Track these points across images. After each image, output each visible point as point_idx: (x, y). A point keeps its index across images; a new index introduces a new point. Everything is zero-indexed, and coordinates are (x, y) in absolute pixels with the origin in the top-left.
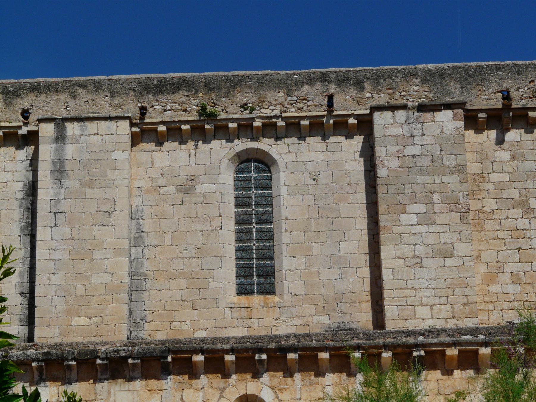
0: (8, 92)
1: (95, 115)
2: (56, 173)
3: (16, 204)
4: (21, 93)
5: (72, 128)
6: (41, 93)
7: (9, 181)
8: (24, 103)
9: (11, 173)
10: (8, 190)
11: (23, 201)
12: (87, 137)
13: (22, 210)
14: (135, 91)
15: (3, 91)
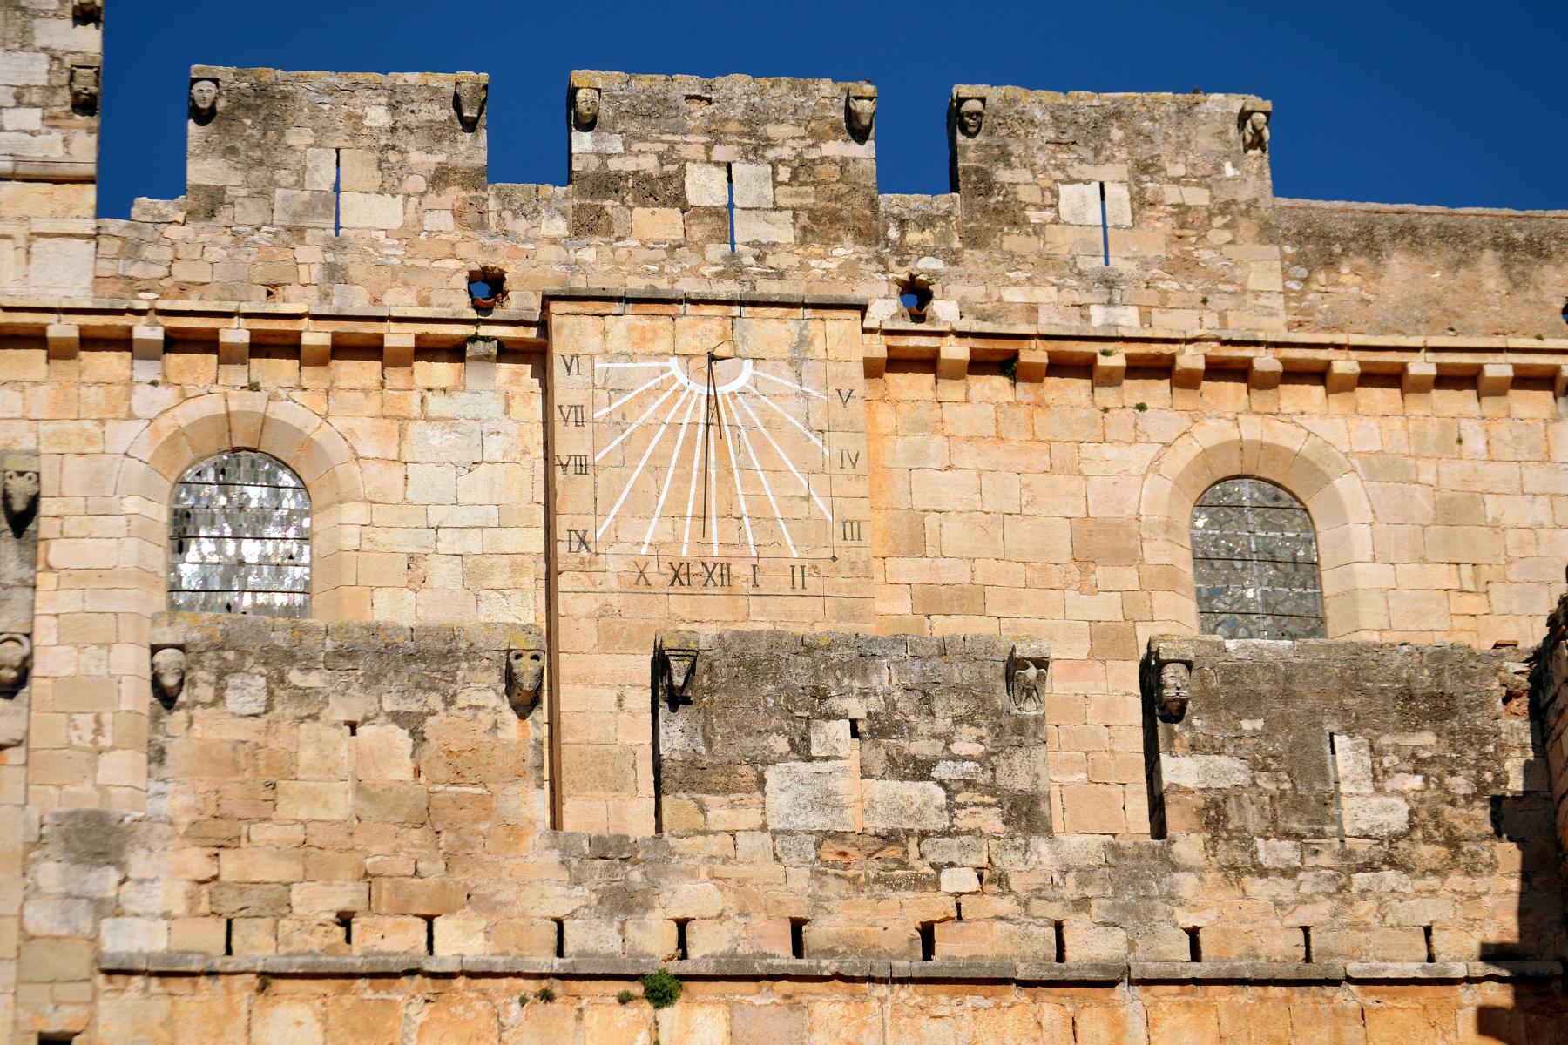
0: (1511, 245)
4: (1553, 248)
7: (1542, 526)
9: (1546, 499)
10: (1543, 554)
15: (1493, 239)
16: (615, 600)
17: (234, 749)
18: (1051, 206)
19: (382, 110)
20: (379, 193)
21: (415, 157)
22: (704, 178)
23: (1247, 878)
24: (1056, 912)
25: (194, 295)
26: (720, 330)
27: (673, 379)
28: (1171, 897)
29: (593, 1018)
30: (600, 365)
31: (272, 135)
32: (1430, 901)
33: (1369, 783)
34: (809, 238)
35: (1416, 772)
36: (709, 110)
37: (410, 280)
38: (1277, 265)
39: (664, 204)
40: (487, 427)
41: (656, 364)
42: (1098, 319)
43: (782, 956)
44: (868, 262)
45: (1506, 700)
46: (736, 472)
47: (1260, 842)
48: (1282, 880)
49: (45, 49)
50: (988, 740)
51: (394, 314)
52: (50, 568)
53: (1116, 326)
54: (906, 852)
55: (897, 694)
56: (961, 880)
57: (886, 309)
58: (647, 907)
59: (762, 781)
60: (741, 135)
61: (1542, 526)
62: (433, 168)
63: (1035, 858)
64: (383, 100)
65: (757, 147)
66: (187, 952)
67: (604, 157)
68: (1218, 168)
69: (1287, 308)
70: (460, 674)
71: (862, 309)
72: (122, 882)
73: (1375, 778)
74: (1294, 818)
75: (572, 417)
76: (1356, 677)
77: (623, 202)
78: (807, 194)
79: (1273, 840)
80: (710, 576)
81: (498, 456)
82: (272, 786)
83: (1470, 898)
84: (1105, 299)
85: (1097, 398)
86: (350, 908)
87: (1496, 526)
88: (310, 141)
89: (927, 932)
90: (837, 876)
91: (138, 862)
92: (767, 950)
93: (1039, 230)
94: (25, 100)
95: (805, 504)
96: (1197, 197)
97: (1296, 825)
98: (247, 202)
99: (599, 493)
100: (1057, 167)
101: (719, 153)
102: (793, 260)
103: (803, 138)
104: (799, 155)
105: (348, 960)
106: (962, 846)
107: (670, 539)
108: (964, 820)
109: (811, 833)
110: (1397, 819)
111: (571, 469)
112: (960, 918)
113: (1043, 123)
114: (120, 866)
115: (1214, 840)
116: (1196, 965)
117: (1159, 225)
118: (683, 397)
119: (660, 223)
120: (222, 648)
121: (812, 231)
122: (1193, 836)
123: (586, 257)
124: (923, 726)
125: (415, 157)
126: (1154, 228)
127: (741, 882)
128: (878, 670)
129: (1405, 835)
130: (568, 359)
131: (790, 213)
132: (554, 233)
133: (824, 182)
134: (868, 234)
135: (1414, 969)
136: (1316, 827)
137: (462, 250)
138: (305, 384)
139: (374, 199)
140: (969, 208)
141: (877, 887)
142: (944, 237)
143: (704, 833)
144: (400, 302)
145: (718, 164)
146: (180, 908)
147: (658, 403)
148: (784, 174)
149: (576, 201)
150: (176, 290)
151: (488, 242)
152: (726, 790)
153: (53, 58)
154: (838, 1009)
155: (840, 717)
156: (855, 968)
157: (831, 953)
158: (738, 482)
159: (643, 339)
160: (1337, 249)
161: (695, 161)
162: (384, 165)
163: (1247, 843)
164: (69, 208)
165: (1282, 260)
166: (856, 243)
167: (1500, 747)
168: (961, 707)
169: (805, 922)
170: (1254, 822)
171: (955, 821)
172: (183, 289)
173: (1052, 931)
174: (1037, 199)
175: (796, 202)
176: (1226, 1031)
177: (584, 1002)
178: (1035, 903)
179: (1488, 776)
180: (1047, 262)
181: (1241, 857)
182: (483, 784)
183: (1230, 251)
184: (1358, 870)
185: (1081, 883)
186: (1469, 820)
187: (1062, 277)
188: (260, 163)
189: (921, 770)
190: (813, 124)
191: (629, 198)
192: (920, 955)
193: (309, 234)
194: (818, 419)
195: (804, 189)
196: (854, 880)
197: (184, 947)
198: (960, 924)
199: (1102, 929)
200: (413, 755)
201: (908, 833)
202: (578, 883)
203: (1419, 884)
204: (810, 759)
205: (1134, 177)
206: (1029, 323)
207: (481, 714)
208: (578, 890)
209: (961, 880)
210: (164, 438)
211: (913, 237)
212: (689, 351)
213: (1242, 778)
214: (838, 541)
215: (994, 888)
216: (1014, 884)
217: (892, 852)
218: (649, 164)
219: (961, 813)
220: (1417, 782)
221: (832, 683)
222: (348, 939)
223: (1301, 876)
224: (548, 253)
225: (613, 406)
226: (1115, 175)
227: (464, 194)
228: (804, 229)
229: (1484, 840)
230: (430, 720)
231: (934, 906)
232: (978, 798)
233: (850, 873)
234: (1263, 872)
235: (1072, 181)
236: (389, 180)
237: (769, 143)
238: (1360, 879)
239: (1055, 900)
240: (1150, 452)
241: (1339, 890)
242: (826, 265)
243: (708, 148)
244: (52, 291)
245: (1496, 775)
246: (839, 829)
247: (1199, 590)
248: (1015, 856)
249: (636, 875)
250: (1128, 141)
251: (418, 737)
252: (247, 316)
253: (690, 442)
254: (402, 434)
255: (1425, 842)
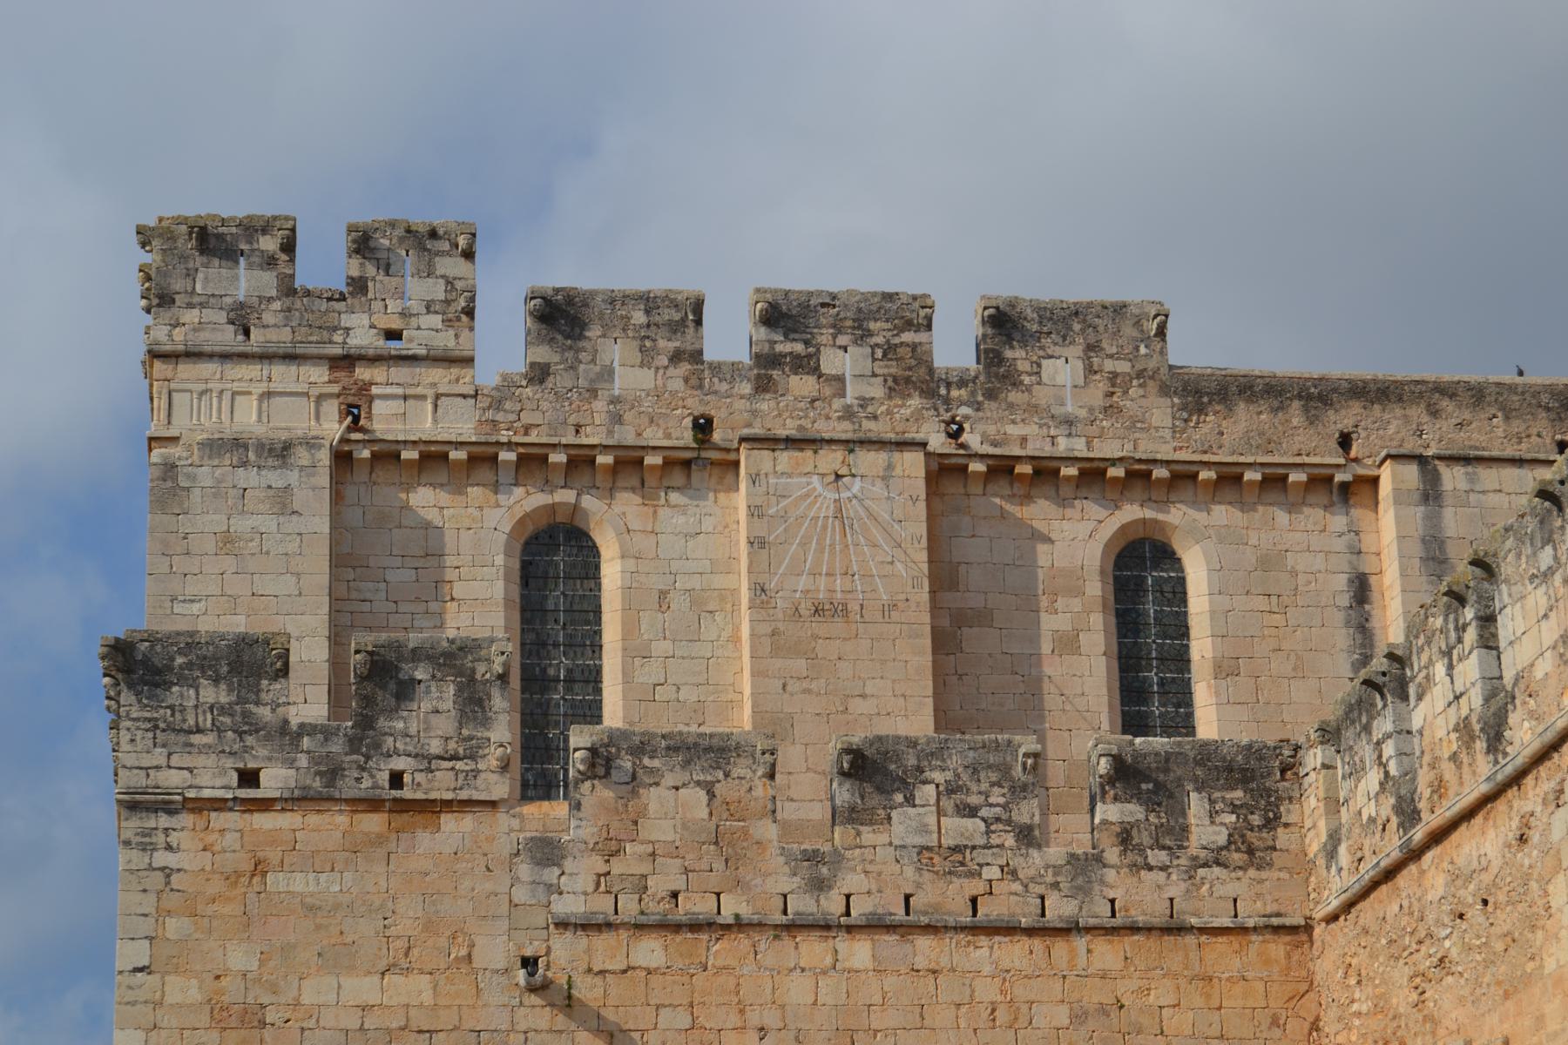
0: (1310, 397)
1: (1486, 454)
2: (1431, 563)
3: (1340, 617)
5: (1453, 478)
6: (1373, 403)
7: (1320, 572)
8: (1343, 417)
11: (1350, 612)
12: (1481, 495)
13: (1351, 631)
14: (1548, 409)
16: (782, 627)
17: (616, 802)
18: (1037, 373)
19: (641, 313)
20: (640, 366)
21: (662, 343)
22: (832, 356)
23: (1143, 873)
24: (1040, 889)
25: (534, 432)
26: (841, 458)
27: (815, 489)
28: (1102, 882)
29: (804, 947)
30: (772, 481)
31: (577, 330)
32: (1237, 884)
33: (1207, 818)
34: (893, 394)
35: (1233, 813)
36: (834, 311)
37: (661, 422)
38: (1169, 410)
39: (808, 373)
40: (704, 511)
41: (804, 480)
42: (1063, 446)
43: (899, 914)
44: (927, 409)
45: (1283, 772)
46: (851, 547)
47: (1149, 851)
48: (1161, 873)
49: (442, 277)
50: (1008, 796)
51: (651, 444)
52: (453, 599)
53: (1073, 450)
54: (964, 858)
55: (960, 770)
56: (992, 873)
57: (938, 441)
58: (830, 888)
59: (889, 818)
60: (854, 328)
61: (1320, 572)
62: (672, 350)
63: (1031, 861)
64: (642, 307)
65: (862, 335)
66: (596, 913)
67: (773, 343)
68: (1137, 349)
69: (1173, 438)
70: (732, 759)
71: (924, 445)
72: (563, 873)
73: (1211, 816)
74: (1168, 838)
75: (756, 513)
76: (1202, 759)
77: (784, 373)
78: (891, 366)
79: (1156, 851)
80: (836, 611)
81: (710, 529)
82: (636, 823)
83: (1258, 882)
84: (1067, 432)
85: (1061, 492)
86: (678, 888)
87: (1294, 573)
88: (599, 333)
89: (974, 901)
90: (928, 870)
91: (569, 865)
92: (892, 911)
93: (1029, 389)
94: (432, 309)
95: (890, 566)
96: (1123, 367)
97: (1168, 842)
98: (563, 373)
99: (772, 561)
100: (1042, 348)
101: (843, 340)
102: (883, 408)
103: (889, 330)
104: (888, 341)
105: (678, 918)
106: (993, 854)
107: (813, 588)
108: (995, 840)
109: (914, 847)
110: (1222, 839)
111: (756, 545)
112: (991, 893)
113: (1033, 319)
114: (559, 865)
115: (1125, 850)
116: (1113, 920)
117: (1101, 384)
118: (820, 499)
119: (802, 385)
120: (608, 746)
121: (895, 390)
122: (1114, 848)
123: (762, 407)
124: (974, 788)
125: (662, 343)
126: (1098, 388)
127: (879, 874)
128: (950, 756)
129: (1226, 848)
130: (754, 476)
131: (882, 378)
132: (742, 392)
133: (902, 359)
134: (929, 392)
135: (1226, 922)
136: (1179, 843)
137: (689, 402)
138: (598, 485)
139: (638, 371)
140: (988, 374)
141: (948, 877)
142: (973, 393)
143: (861, 847)
144: (653, 437)
145: (840, 347)
146: (590, 889)
147: (806, 504)
148: (879, 353)
149: (755, 372)
150: (522, 430)
151: (702, 397)
152: (871, 823)
153: (448, 282)
154: (928, 943)
155: (930, 783)
156: (938, 921)
157: (925, 913)
158: (852, 552)
159: (797, 464)
160: (1205, 399)
161: (825, 345)
162: (643, 349)
163: (1141, 850)
164: (457, 380)
165: (1172, 407)
166: (921, 397)
167: (1279, 799)
168: (994, 777)
169: (911, 895)
170: (1146, 840)
171: (991, 840)
172: (527, 430)
173: (1039, 901)
174: (1028, 369)
175: (886, 371)
176: (1129, 955)
177: (797, 940)
178: (1031, 886)
179: (1271, 815)
180: (1034, 409)
181: (1140, 860)
182: (743, 820)
183: (1144, 402)
184: (1200, 867)
185: (1055, 874)
186: (1261, 839)
187: (1042, 418)
188: (570, 348)
189: (972, 812)
190: (896, 321)
191: (787, 369)
192: (971, 914)
193: (599, 393)
194: (898, 514)
195: (890, 363)
196: (937, 873)
197: (594, 910)
198: (991, 897)
199: (1065, 899)
200: (708, 805)
201: (966, 847)
202: (795, 875)
203: (1233, 875)
204: (914, 806)
205: (1086, 354)
206: (1022, 448)
207: (743, 782)
208: (795, 879)
209: (992, 873)
210: (517, 518)
211: (955, 393)
212: (825, 471)
213: (1141, 816)
214: (909, 589)
215: (1010, 877)
216: (1021, 876)
217: (959, 857)
218: (799, 348)
219: (993, 836)
220: (1233, 818)
221: (926, 763)
222: (677, 906)
223: (1170, 870)
224: (740, 405)
225: (780, 505)
226: (1075, 351)
227: (689, 367)
228: (890, 388)
229: (1267, 850)
230: (717, 785)
231: (977, 887)
232: (1001, 826)
233: (935, 869)
234: (1150, 868)
235: (1051, 357)
236: (647, 356)
237: (870, 334)
238: (1201, 872)
239: (1041, 883)
240: (1092, 525)
241: (1190, 878)
242: (902, 411)
243: (835, 337)
244: (451, 430)
245: (1275, 814)
246: (929, 844)
247: (1117, 609)
248: (1021, 859)
249: (824, 870)
250: (1083, 330)
251: (711, 795)
252: (565, 446)
253: (825, 527)
254: (655, 512)
255: (1236, 851)
